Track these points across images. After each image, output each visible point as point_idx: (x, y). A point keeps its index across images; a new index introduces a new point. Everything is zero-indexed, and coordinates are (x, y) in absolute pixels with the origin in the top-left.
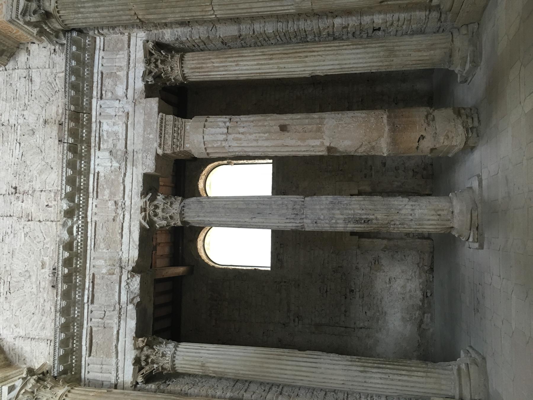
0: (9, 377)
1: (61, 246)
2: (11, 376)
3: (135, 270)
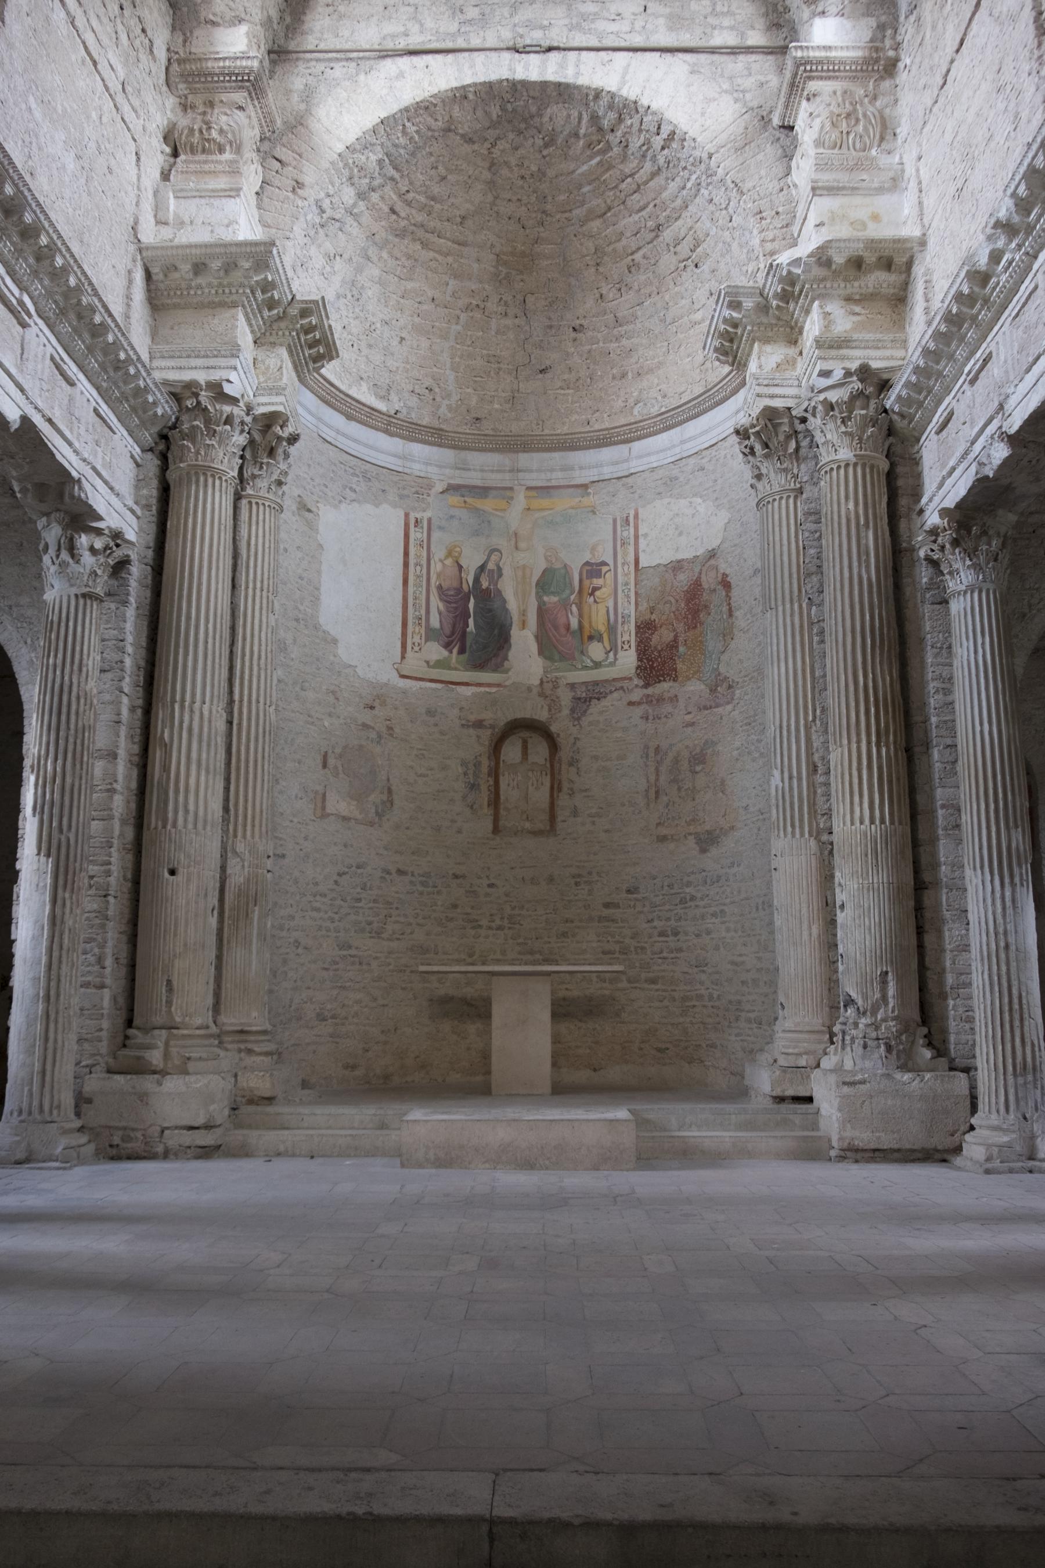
0: (854, 344)
1: (966, 268)
2: (854, 344)
3: (1013, 440)
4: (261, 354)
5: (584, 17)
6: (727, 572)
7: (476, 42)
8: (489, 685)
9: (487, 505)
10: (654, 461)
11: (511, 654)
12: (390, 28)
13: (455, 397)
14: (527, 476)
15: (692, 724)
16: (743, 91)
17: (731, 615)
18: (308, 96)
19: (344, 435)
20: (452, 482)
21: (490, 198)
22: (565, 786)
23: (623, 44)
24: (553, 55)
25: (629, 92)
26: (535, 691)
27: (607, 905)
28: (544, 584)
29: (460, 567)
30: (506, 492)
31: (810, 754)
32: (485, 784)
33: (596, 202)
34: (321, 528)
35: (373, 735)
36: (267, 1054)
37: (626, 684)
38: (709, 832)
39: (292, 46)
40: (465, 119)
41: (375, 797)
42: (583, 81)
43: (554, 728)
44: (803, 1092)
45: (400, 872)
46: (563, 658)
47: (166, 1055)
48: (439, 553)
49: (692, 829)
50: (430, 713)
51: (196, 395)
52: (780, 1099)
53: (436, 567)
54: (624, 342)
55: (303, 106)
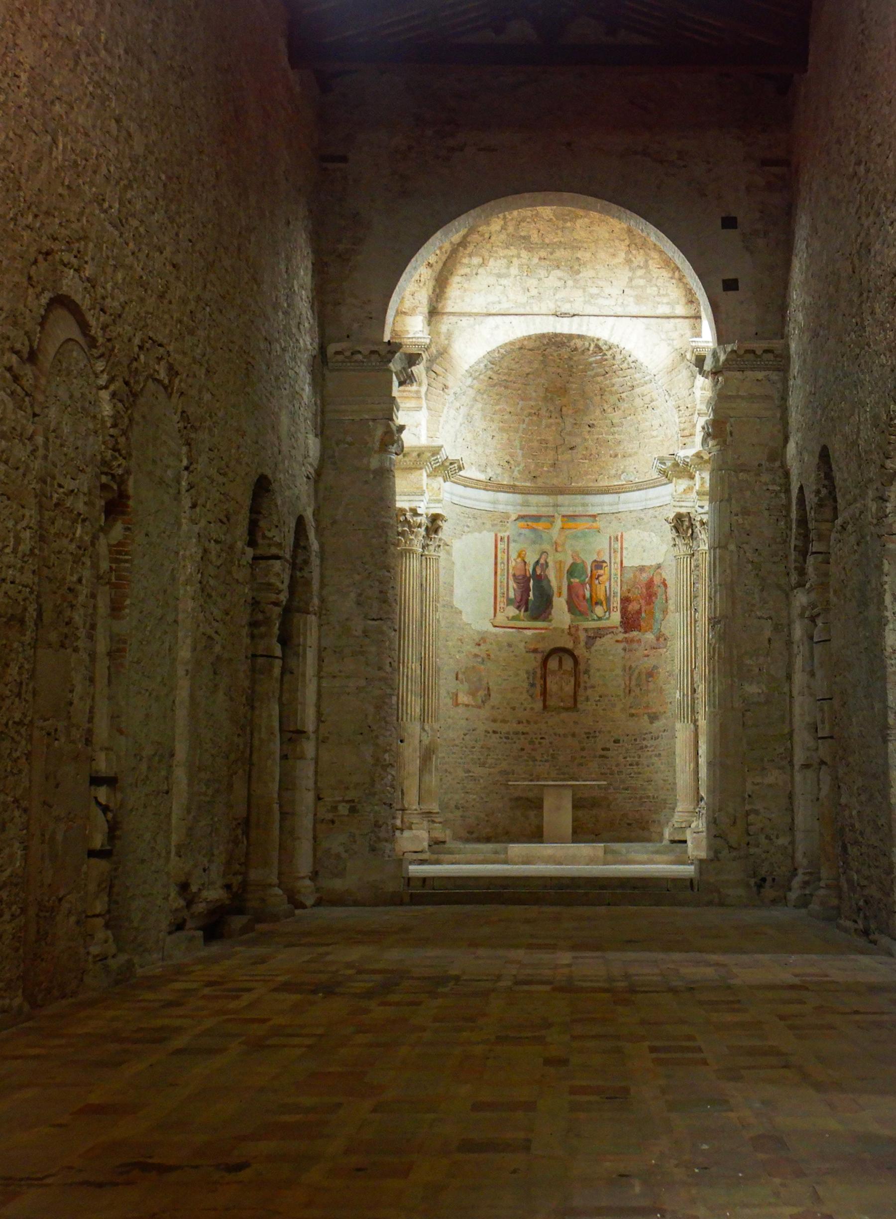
4: (430, 482)
5: (592, 296)
6: (666, 578)
7: (536, 310)
8: (541, 629)
9: (540, 526)
10: (631, 507)
11: (553, 611)
12: (492, 298)
13: (522, 465)
14: (562, 509)
15: (648, 656)
16: (673, 340)
17: (666, 601)
18: (449, 335)
19: (464, 498)
20: (522, 513)
21: (542, 366)
22: (582, 685)
23: (612, 313)
24: (576, 318)
25: (614, 340)
26: (566, 632)
27: (603, 749)
28: (571, 573)
29: (525, 563)
30: (551, 518)
31: (692, 684)
32: (539, 683)
33: (601, 371)
34: (454, 554)
35: (480, 660)
36: (440, 823)
37: (614, 630)
38: (655, 713)
39: (439, 309)
40: (531, 345)
41: (482, 693)
42: (591, 334)
43: (576, 653)
44: (682, 838)
45: (494, 732)
46: (582, 614)
47: (402, 822)
48: (514, 555)
49: (646, 711)
50: (510, 645)
51: (405, 515)
52: (673, 842)
53: (512, 564)
54: (617, 436)
55: (446, 342)
